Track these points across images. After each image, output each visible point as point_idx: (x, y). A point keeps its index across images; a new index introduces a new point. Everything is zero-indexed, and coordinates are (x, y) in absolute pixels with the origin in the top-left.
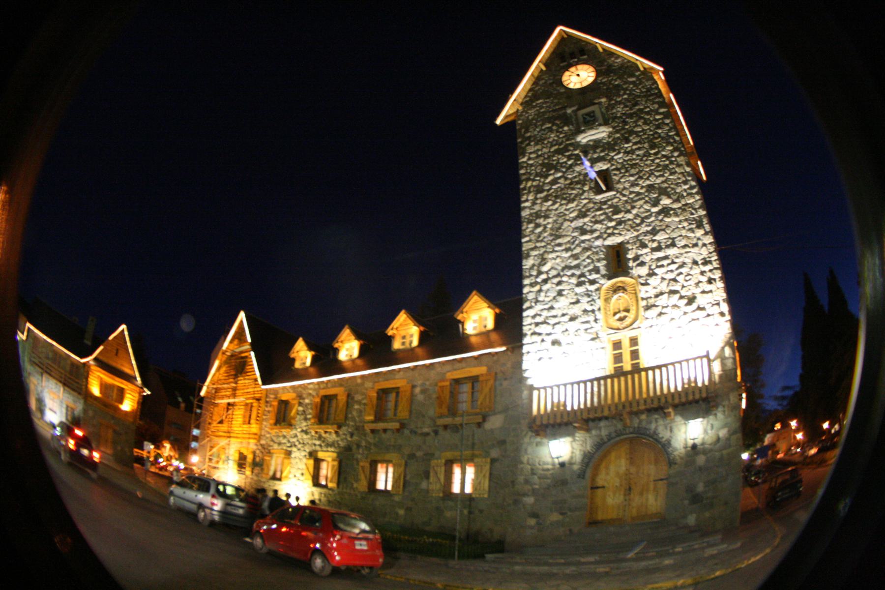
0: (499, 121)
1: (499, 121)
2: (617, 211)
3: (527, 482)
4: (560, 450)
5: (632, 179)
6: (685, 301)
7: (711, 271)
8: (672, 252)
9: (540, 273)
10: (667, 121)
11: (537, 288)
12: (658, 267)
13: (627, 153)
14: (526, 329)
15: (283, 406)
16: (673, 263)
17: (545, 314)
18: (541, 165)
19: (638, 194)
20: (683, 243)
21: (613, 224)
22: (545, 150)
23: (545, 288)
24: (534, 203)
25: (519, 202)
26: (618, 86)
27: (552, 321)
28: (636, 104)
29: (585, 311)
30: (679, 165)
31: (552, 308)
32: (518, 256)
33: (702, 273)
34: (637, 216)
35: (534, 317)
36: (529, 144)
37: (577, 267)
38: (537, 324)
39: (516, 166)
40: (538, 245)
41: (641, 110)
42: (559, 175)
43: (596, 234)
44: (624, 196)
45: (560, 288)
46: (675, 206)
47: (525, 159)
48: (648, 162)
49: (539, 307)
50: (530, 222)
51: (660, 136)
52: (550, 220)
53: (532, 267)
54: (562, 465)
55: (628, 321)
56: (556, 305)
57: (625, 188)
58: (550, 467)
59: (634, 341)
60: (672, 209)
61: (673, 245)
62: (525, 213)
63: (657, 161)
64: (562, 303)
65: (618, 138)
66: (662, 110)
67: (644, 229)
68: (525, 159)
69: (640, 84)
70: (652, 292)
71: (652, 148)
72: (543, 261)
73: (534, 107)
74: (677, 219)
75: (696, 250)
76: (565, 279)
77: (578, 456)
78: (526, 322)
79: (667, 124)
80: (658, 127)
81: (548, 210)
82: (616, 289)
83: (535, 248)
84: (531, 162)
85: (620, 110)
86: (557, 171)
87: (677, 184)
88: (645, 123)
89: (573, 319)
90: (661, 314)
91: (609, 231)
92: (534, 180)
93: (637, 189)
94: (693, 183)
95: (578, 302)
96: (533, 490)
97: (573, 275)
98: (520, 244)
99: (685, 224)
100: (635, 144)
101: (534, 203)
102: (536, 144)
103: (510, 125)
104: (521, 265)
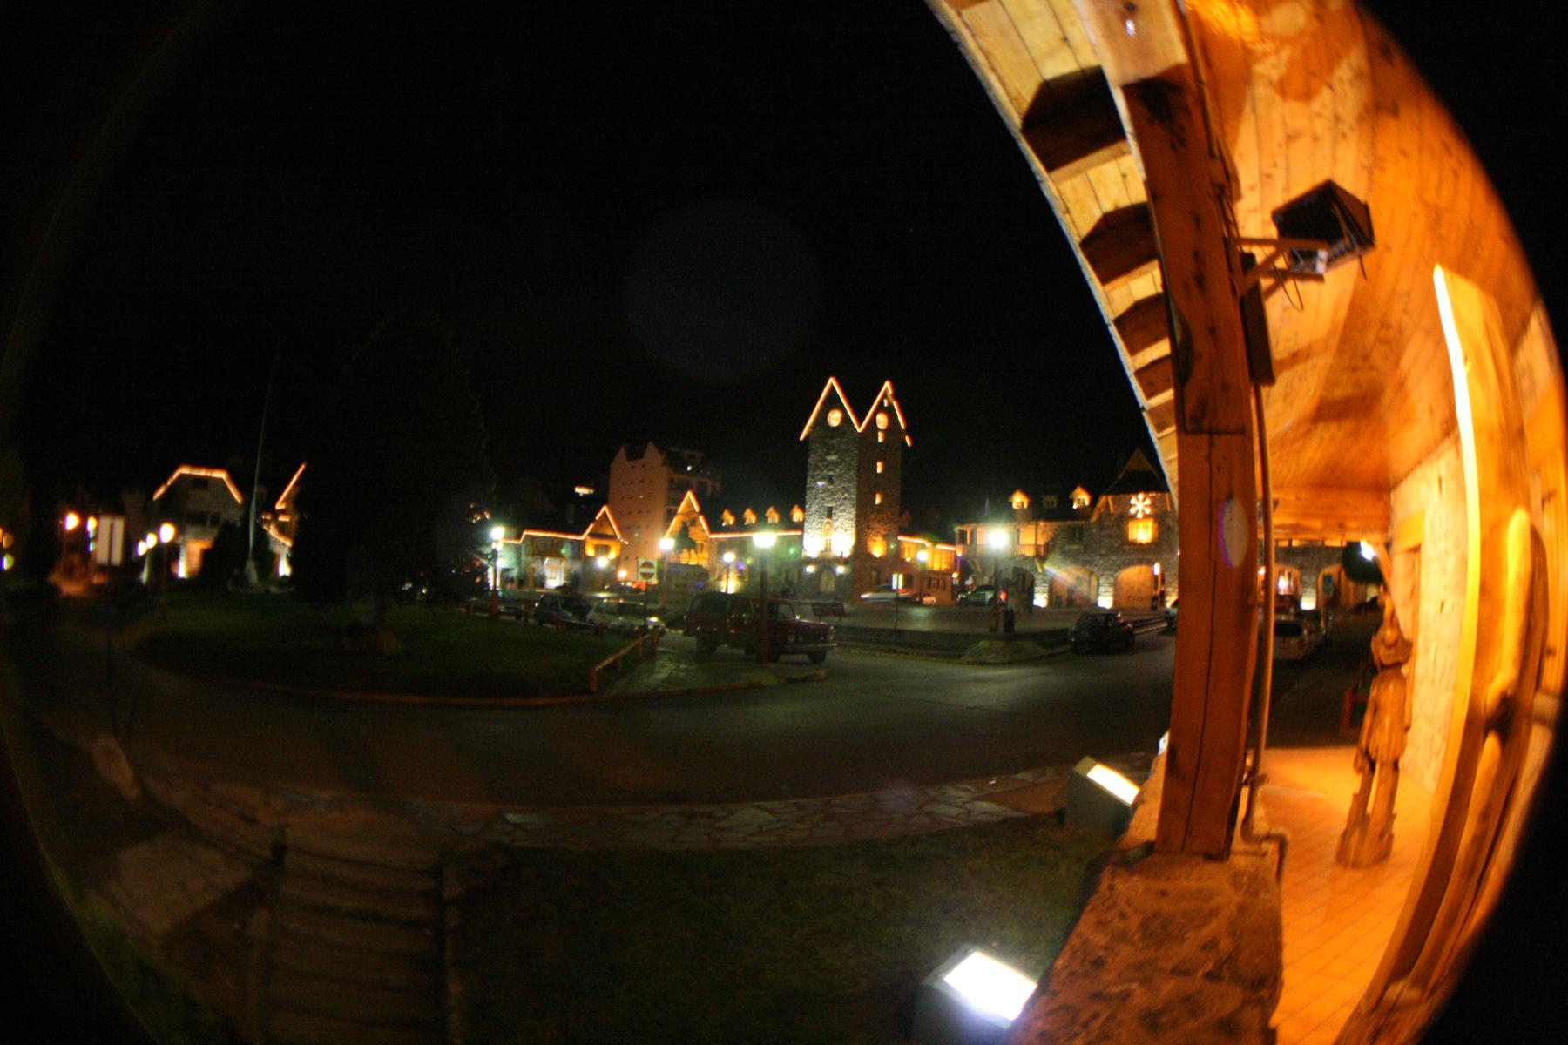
4: (810, 569)
39: (806, 463)
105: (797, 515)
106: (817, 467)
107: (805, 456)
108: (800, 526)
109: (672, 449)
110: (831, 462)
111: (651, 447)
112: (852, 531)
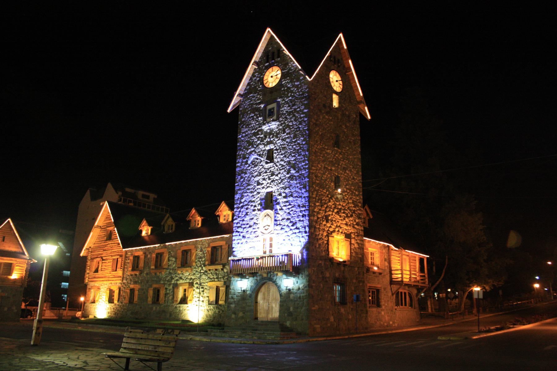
0: (229, 111)
1: (229, 111)
2: (273, 174)
3: (232, 298)
5: (282, 156)
6: (292, 224)
7: (304, 211)
8: (291, 199)
9: (241, 203)
10: (306, 119)
11: (239, 210)
12: (284, 206)
13: (283, 140)
14: (234, 228)
15: (136, 259)
16: (290, 205)
17: (241, 222)
18: (247, 141)
19: (283, 166)
20: (295, 195)
21: (269, 181)
22: (249, 132)
23: (242, 210)
24: (241, 165)
25: (236, 163)
26: (289, 88)
27: (243, 226)
28: (294, 105)
29: (255, 223)
30: (303, 150)
31: (243, 220)
32: (233, 193)
33: (301, 211)
34: (280, 178)
35: (237, 223)
36: (242, 127)
37: (254, 201)
38: (238, 227)
39: (236, 140)
40: (241, 188)
41: (295, 109)
42: (253, 149)
43: (263, 186)
44: (277, 166)
45: (247, 211)
46: (296, 175)
47: (240, 136)
48: (291, 147)
49: (239, 219)
50: (239, 175)
51: (299, 130)
52: (247, 175)
53: (238, 200)
54: (244, 291)
55: (268, 231)
56: (245, 219)
57: (278, 162)
58: (240, 291)
59: (271, 239)
60: (295, 176)
61: (292, 196)
62: (238, 169)
63: (294, 147)
65: (281, 129)
66: (306, 111)
67: (282, 186)
68: (240, 136)
69: (300, 87)
70: (280, 218)
72: (242, 197)
73: (248, 99)
74: (295, 182)
75: (300, 199)
76: (249, 207)
77: (249, 288)
78: (235, 225)
79: (305, 121)
80: (300, 124)
81: (246, 169)
83: (240, 190)
84: (242, 139)
86: (253, 147)
87: (300, 162)
88: (295, 120)
89: (250, 227)
90: (282, 229)
91: (268, 185)
92: (243, 151)
93: (282, 163)
94: (307, 162)
95: (252, 219)
96: (235, 301)
97: (252, 206)
98: (235, 186)
99: (298, 185)
100: (287, 134)
101: (241, 165)
102: (246, 127)
103: (236, 110)
104: (234, 198)
105: (224, 213)
107: (235, 131)
108: (228, 229)
109: (127, 190)
110: (271, 133)
111: (110, 188)
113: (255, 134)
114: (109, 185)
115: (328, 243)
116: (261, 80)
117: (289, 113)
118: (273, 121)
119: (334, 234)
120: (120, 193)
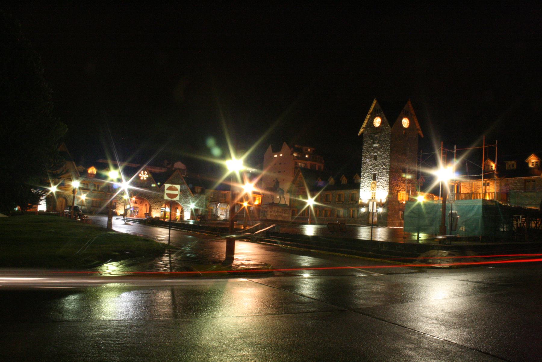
32: (360, 172)
39: (362, 149)
64: (366, 183)
71: (385, 152)
82: (373, 183)
85: (382, 138)
103: (362, 134)
106: (368, 151)
107: (362, 145)
110: (376, 148)
112: (387, 188)
113: (370, 147)
114: (285, 143)
115: (397, 195)
116: (372, 122)
117: (384, 141)
118: (377, 143)
119: (401, 192)
120: (292, 149)
